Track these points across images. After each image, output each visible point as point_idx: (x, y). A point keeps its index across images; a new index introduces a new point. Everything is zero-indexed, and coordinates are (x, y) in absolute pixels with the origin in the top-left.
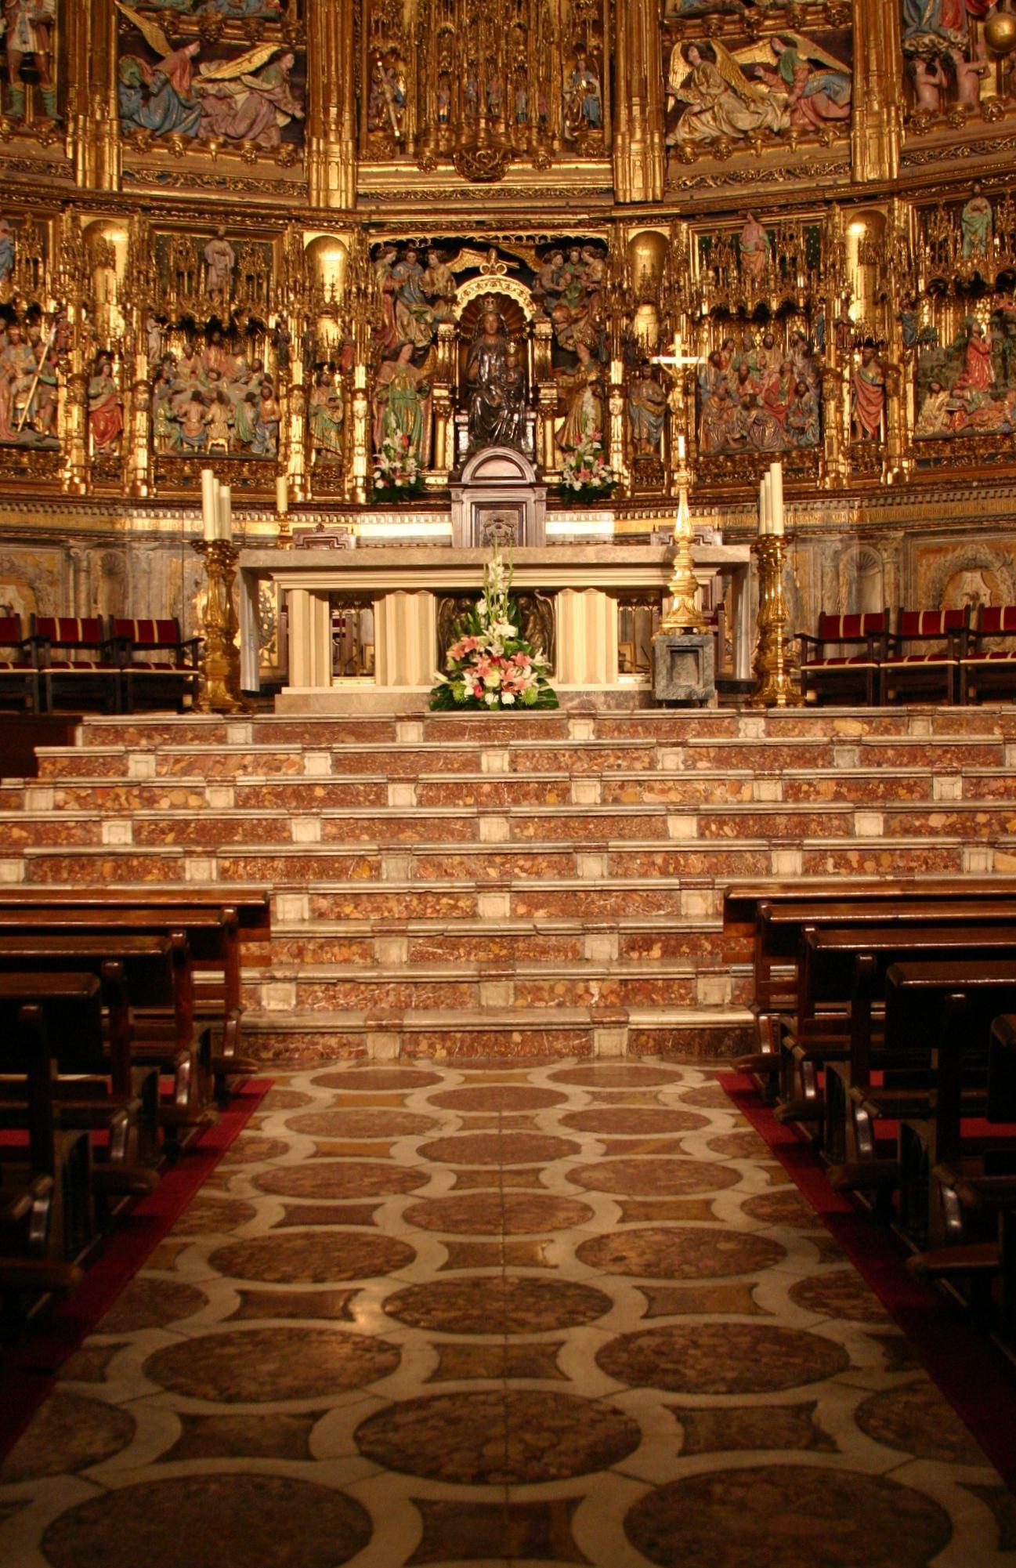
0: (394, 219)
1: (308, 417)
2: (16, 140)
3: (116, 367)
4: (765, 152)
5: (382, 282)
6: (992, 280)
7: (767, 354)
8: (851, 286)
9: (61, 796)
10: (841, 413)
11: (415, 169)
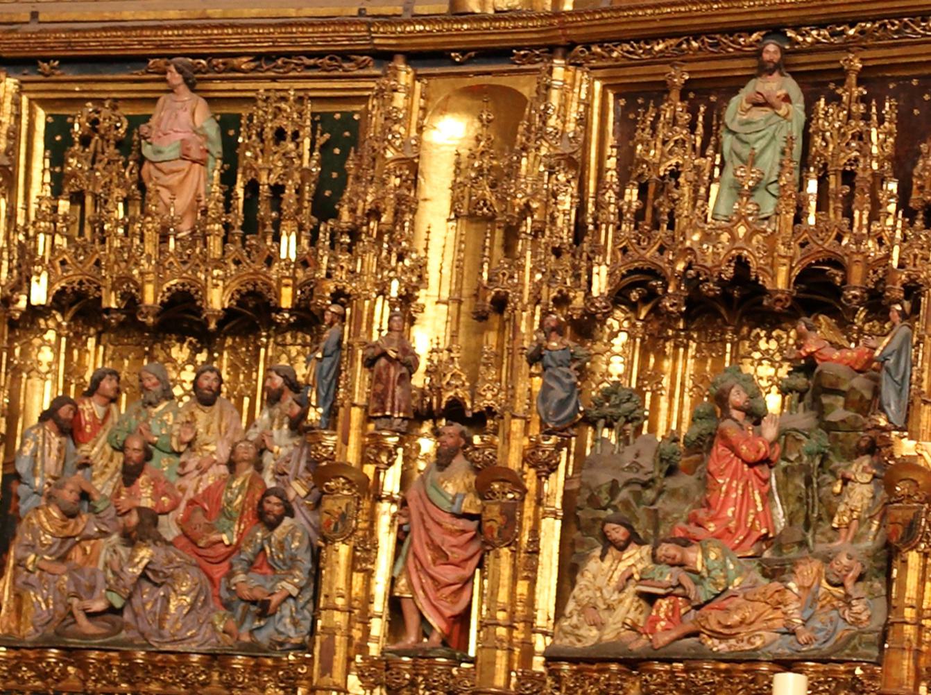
7: (201, 416)
8: (420, 268)
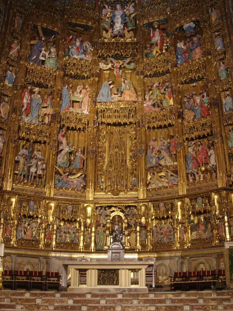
0: (100, 202)
1: (84, 236)
2: (37, 188)
3: (51, 227)
4: (164, 190)
5: (98, 213)
6: (202, 211)
9: (23, 306)
10: (178, 235)
11: (104, 194)
